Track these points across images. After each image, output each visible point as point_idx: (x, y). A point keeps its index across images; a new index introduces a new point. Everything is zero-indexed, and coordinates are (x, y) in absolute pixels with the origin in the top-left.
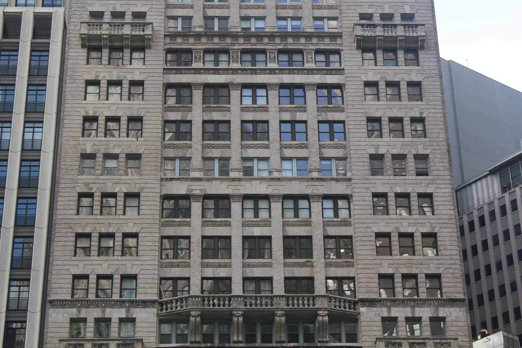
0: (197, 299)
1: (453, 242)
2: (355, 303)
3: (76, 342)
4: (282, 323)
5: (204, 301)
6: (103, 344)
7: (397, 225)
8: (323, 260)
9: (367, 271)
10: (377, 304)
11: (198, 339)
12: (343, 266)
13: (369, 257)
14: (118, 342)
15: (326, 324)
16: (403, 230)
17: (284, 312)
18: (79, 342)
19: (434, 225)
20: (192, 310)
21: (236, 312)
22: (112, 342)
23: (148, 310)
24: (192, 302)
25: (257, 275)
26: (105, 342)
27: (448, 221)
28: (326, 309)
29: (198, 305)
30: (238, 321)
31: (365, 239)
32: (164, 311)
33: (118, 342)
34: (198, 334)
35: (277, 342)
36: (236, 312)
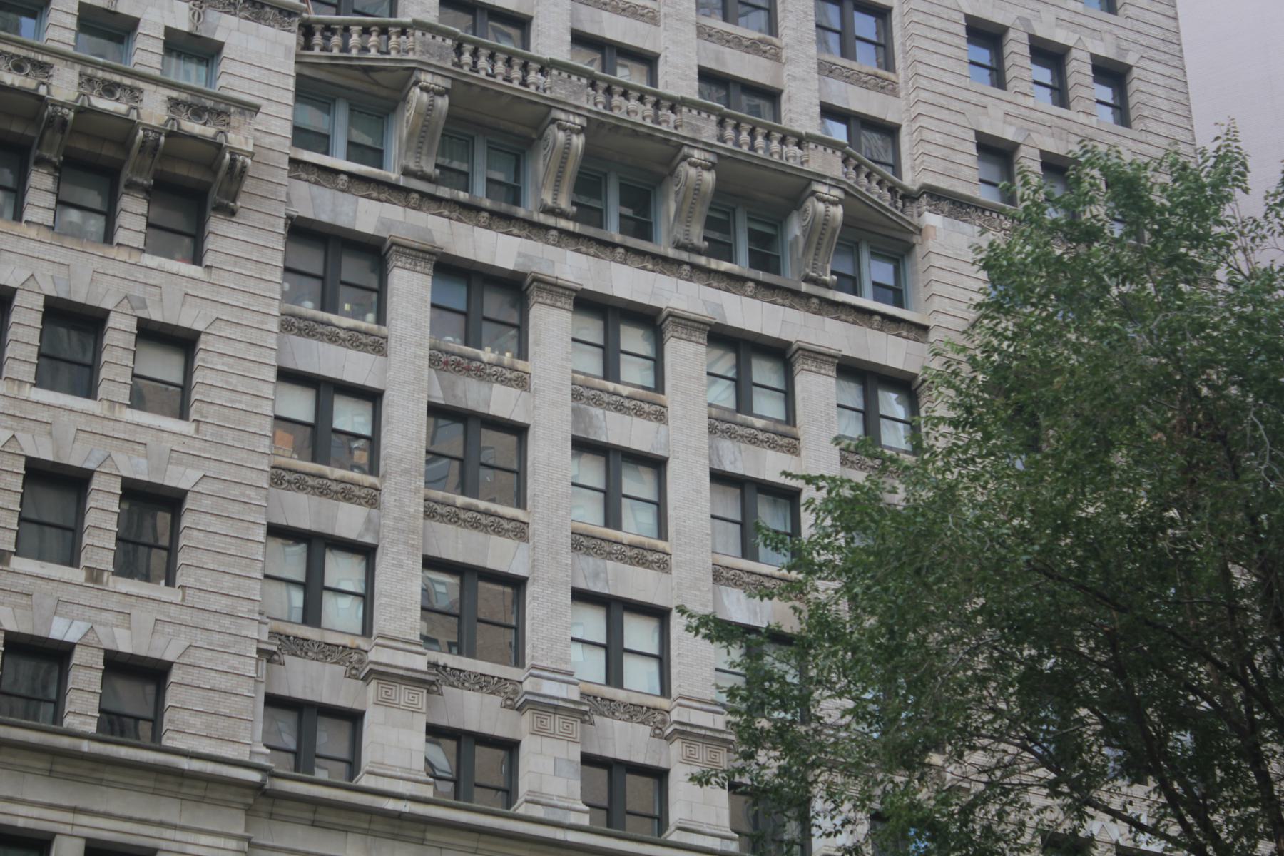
0: (439, 39)
1: (1176, 106)
2: (909, 197)
3: (23, 53)
4: (703, 188)
5: (459, 50)
6: (119, 85)
7: (1026, 13)
8: (813, 50)
9: (944, 114)
10: (974, 215)
11: (429, 168)
12: (864, 85)
13: (948, 78)
14: (174, 94)
15: (834, 230)
16: (1041, 32)
17: (712, 158)
18: (32, 55)
19: (1124, 44)
20: (424, 67)
21: (562, 116)
22: (152, 87)
23: (264, 29)
24: (424, 44)
25: (610, 34)
26: (127, 81)
27: (1161, 46)
28: (837, 183)
29: (441, 57)
30: (568, 144)
31: (936, 22)
32: (317, 51)
33: (174, 94)
34: (429, 154)
35: (679, 246)
36: (562, 116)
